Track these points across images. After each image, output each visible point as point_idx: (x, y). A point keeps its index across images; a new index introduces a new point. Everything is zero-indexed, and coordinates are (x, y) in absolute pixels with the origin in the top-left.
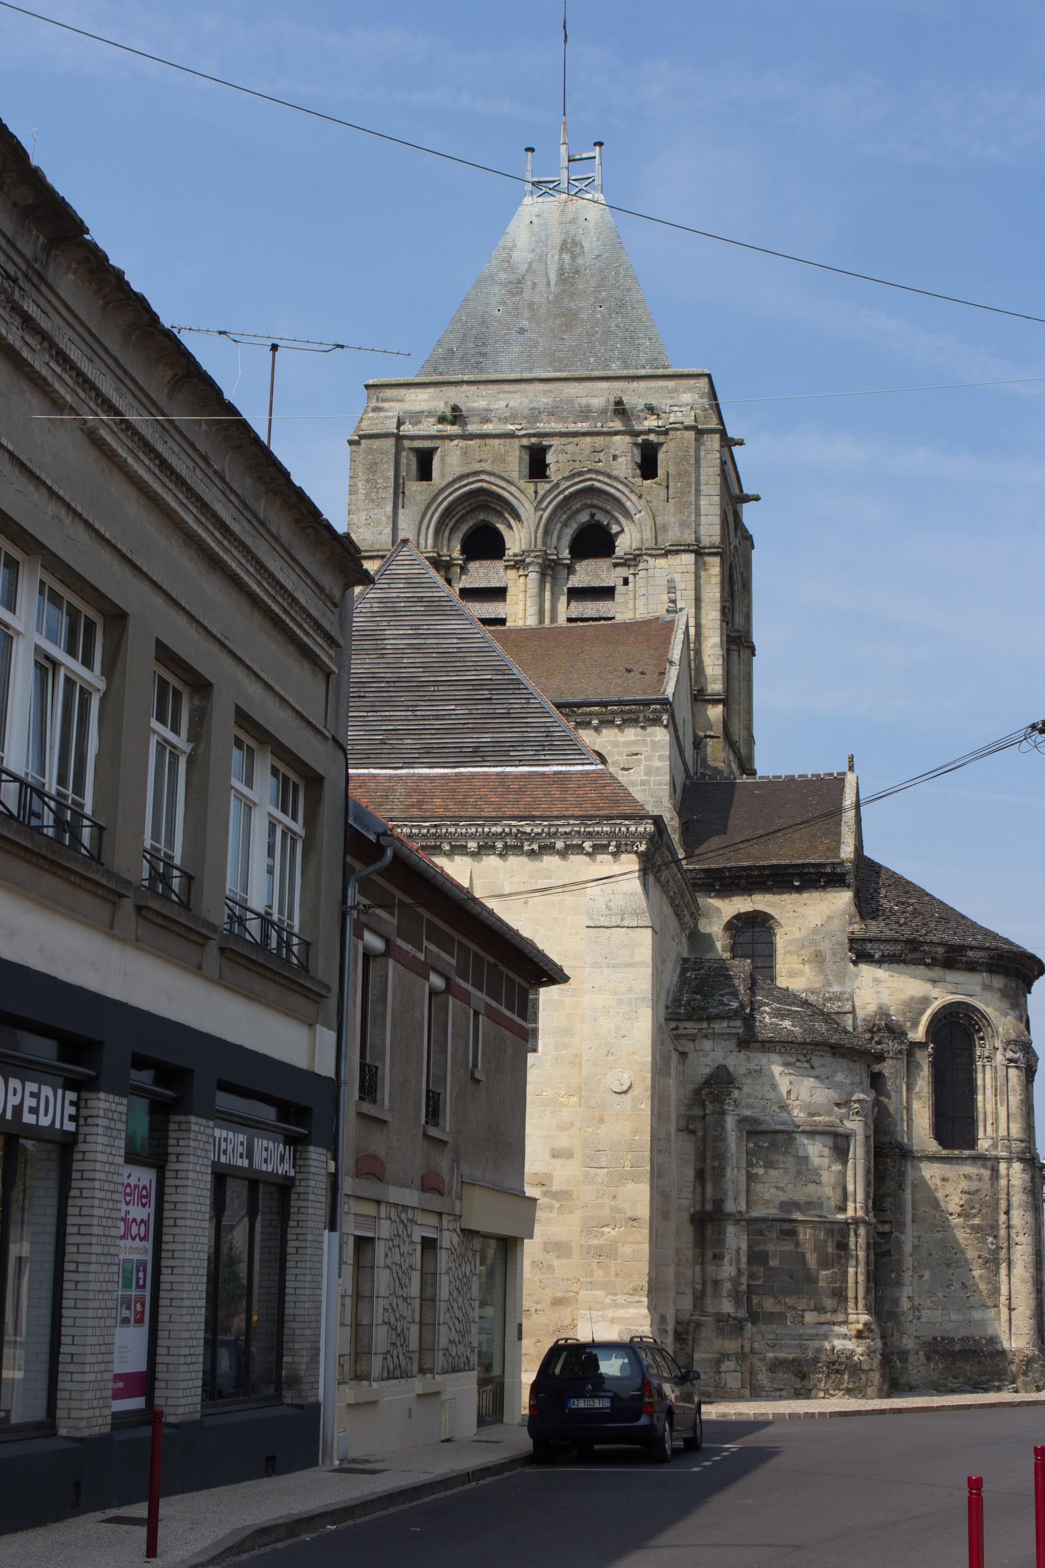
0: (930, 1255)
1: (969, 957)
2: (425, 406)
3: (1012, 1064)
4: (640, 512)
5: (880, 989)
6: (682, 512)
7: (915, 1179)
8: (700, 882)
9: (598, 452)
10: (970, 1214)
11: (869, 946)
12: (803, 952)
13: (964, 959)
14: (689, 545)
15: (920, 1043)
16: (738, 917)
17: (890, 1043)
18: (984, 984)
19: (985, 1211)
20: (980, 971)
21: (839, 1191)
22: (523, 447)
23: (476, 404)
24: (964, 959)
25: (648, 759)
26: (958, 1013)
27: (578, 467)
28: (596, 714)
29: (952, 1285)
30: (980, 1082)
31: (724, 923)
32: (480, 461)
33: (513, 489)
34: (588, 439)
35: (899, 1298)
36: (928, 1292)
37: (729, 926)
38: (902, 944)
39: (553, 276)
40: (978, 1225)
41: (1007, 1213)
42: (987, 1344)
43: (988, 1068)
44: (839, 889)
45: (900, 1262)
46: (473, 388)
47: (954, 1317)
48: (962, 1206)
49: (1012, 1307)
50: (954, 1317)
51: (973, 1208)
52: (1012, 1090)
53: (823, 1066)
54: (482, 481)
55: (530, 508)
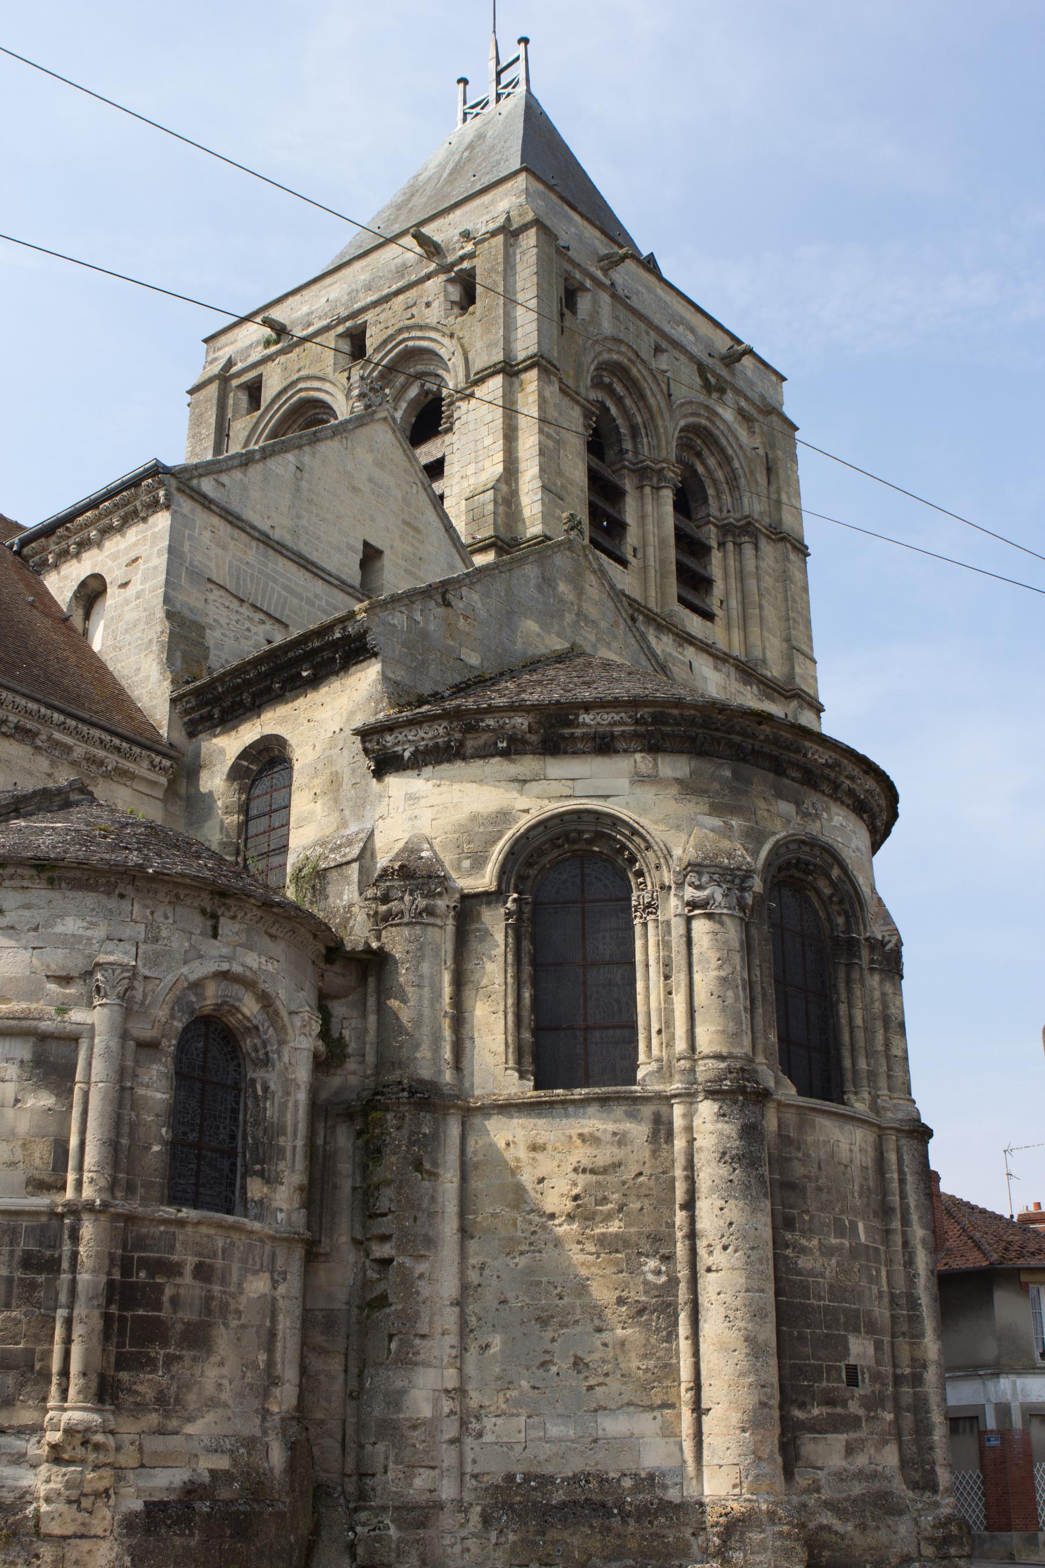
0: (504, 1302)
1: (584, 724)
2: (254, 338)
3: (697, 912)
4: (453, 354)
5: (417, 812)
6: (489, 331)
7: (475, 1153)
8: (195, 715)
9: (411, 307)
10: (595, 1213)
11: (389, 739)
12: (316, 781)
13: (578, 732)
14: (495, 365)
15: (486, 894)
16: (245, 754)
17: (407, 898)
18: (637, 774)
19: (635, 1206)
20: (625, 751)
21: (41, 1154)
22: (340, 336)
23: (299, 313)
24: (578, 732)
25: (148, 560)
26: (580, 833)
27: (390, 332)
28: (92, 523)
29: (551, 1362)
30: (639, 957)
31: (226, 770)
32: (299, 370)
33: (327, 386)
34: (401, 297)
35: (403, 1392)
36: (498, 1378)
37: (236, 773)
38: (445, 724)
39: (445, 175)
40: (617, 1235)
41: (690, 1205)
42: (637, 1488)
43: (651, 925)
44: (365, 664)
45: (410, 1318)
46: (297, 297)
47: (555, 1430)
48: (576, 1198)
49: (704, 1406)
50: (555, 1430)
51: (605, 1200)
52: (700, 961)
53: (27, 906)
54: (301, 390)
55: (341, 397)
